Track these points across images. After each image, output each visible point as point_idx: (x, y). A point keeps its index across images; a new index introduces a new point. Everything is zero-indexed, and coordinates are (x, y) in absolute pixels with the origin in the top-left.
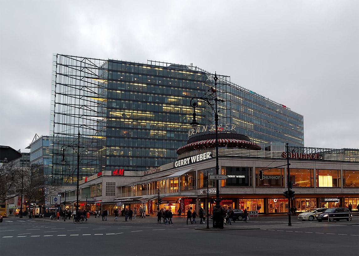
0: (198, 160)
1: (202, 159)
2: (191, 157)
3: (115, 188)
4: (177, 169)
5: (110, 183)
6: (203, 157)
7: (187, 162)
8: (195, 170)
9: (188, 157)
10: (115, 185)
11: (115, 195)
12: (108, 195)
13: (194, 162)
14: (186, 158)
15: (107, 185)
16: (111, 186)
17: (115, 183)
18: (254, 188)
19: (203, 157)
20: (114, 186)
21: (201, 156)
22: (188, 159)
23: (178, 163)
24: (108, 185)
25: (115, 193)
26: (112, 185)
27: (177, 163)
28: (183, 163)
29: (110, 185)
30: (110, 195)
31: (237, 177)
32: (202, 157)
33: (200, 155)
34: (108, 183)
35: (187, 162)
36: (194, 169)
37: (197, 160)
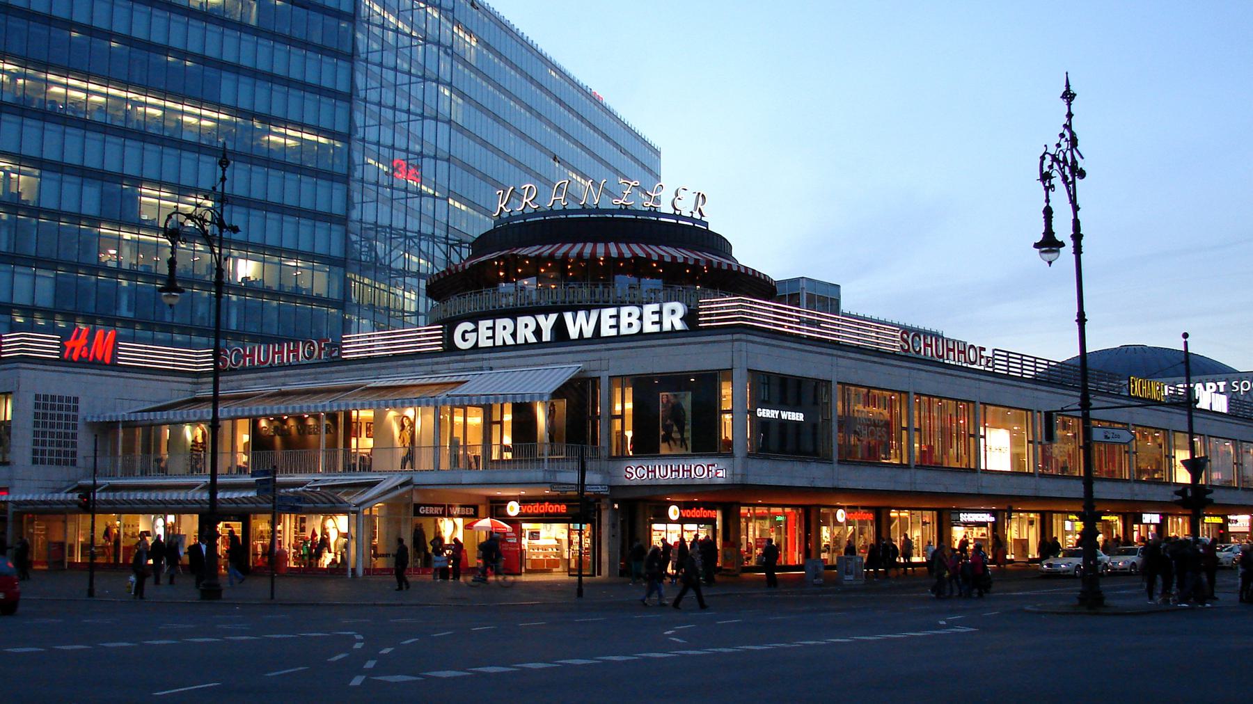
0: (613, 332)
1: (635, 330)
2: (568, 316)
3: (75, 427)
4: (467, 357)
5: (53, 398)
6: (641, 318)
7: (538, 332)
8: (595, 374)
9: (546, 311)
10: (76, 409)
11: (74, 463)
12: (43, 462)
13: (588, 333)
14: (533, 312)
15: (37, 406)
16: (60, 417)
17: (76, 400)
18: (836, 465)
19: (641, 318)
20: (71, 413)
21: (630, 315)
22: (547, 323)
23: (476, 330)
24: (45, 407)
25: (74, 454)
26: (60, 408)
27: (466, 332)
28: (514, 335)
29: (53, 408)
30: (51, 462)
31: (784, 415)
32: (634, 320)
33: (625, 311)
34: (45, 398)
35: (538, 332)
36: (594, 365)
37: (606, 331)
